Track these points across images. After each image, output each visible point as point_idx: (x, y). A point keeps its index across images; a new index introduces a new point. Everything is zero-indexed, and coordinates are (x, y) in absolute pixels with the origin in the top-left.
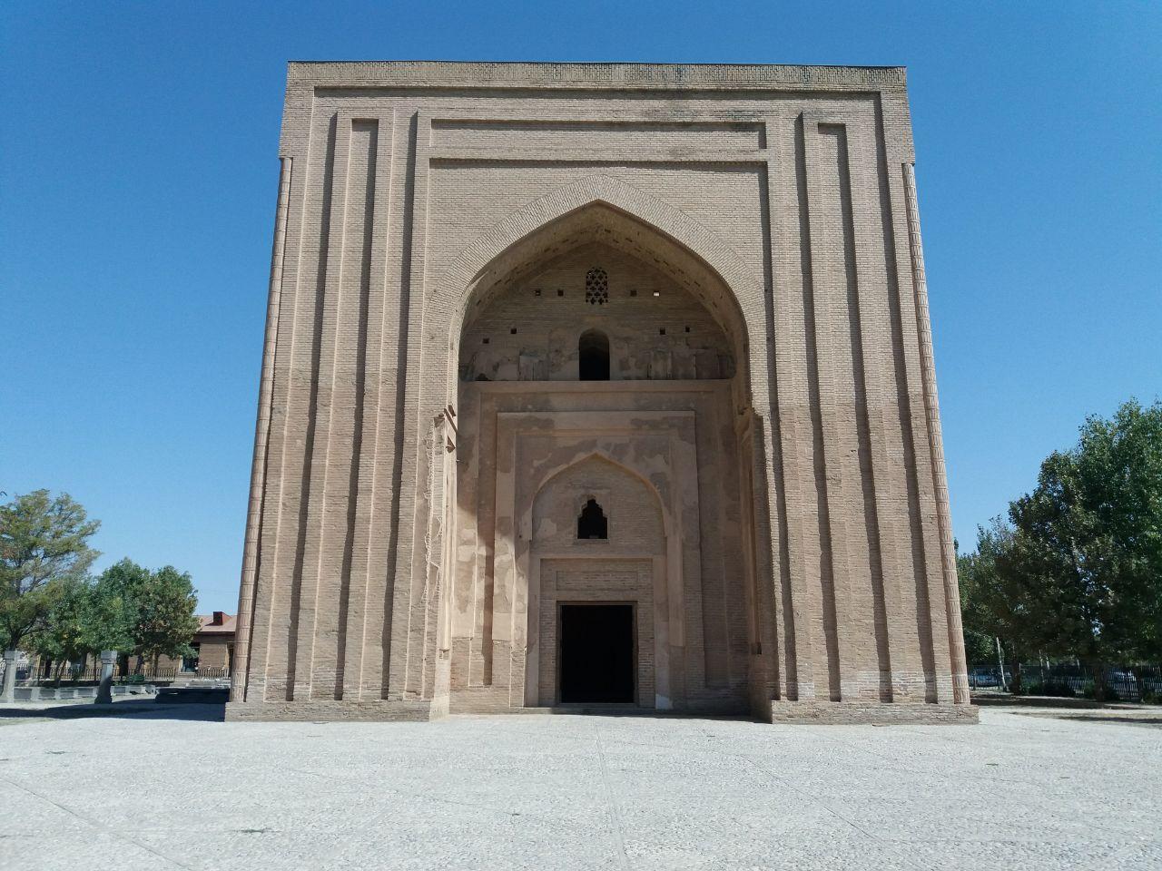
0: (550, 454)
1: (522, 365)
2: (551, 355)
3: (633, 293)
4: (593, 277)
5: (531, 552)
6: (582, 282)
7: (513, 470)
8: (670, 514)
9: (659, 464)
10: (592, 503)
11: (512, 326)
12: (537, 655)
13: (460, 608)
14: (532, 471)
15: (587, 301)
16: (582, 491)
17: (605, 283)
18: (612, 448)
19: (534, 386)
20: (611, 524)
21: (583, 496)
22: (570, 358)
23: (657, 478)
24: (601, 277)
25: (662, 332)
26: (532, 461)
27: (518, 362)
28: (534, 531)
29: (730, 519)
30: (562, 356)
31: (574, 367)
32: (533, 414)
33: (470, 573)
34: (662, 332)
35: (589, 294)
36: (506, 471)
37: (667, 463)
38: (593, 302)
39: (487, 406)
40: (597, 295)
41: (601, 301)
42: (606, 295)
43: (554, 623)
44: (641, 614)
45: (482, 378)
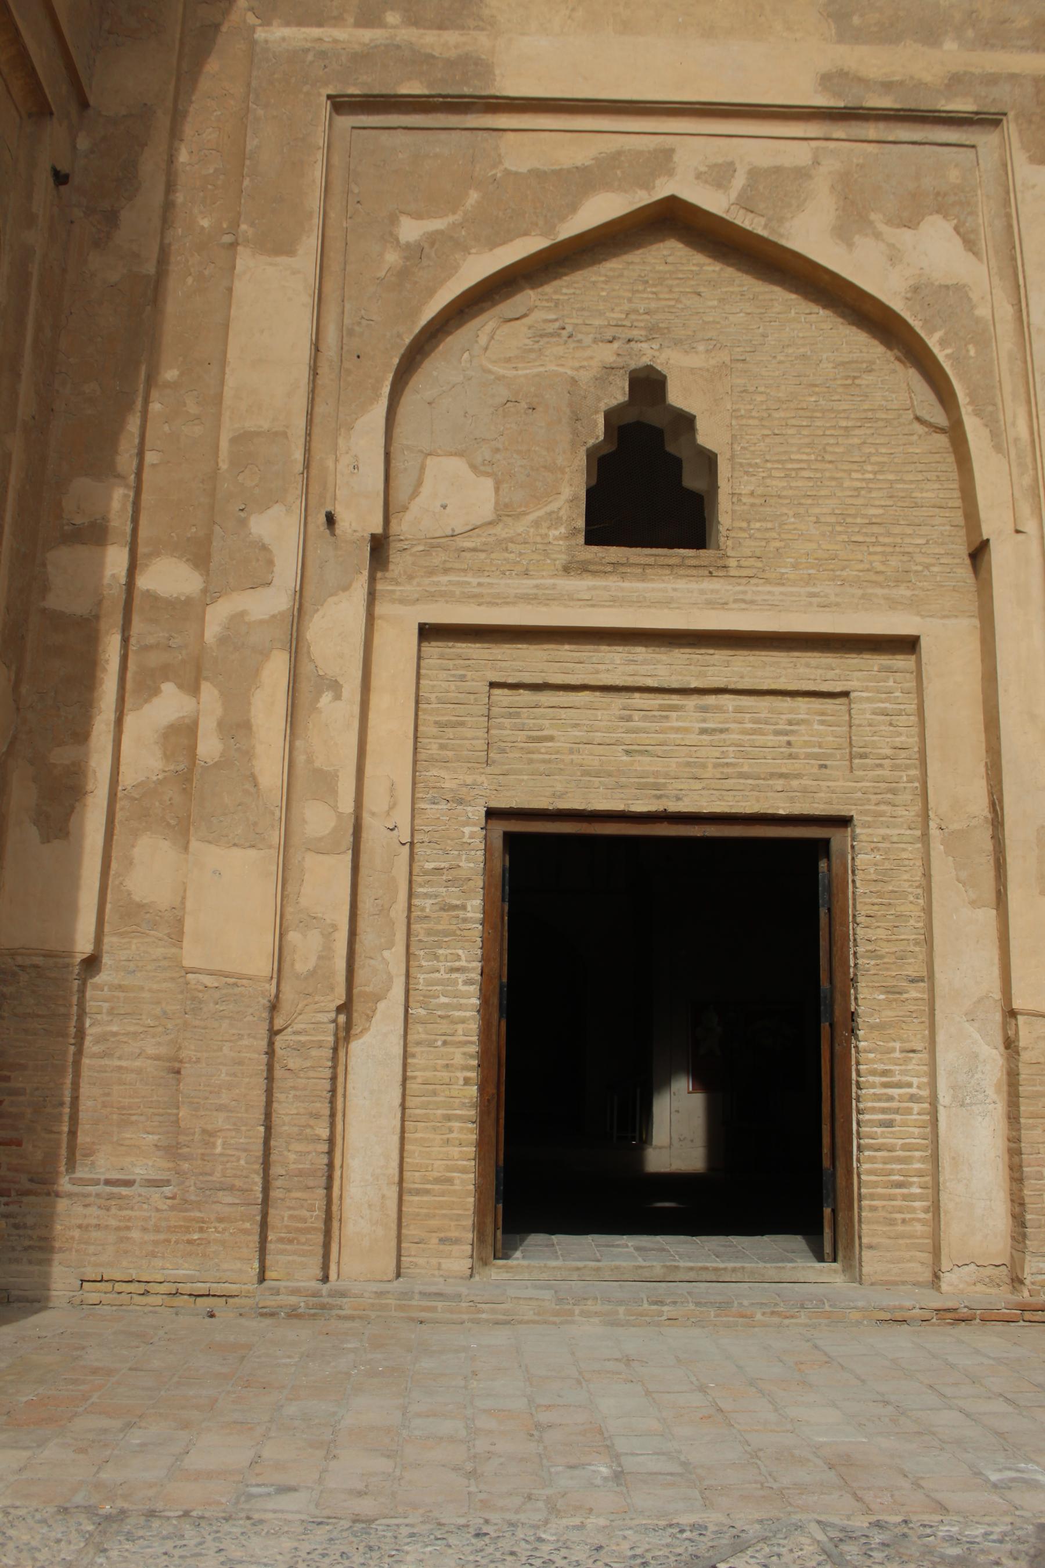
0: (474, 196)
7: (311, 243)
8: (998, 448)
10: (648, 385)
14: (392, 258)
16: (607, 354)
18: (739, 181)
26: (393, 220)
36: (280, 246)
37: (970, 244)
43: (474, 907)
44: (874, 882)
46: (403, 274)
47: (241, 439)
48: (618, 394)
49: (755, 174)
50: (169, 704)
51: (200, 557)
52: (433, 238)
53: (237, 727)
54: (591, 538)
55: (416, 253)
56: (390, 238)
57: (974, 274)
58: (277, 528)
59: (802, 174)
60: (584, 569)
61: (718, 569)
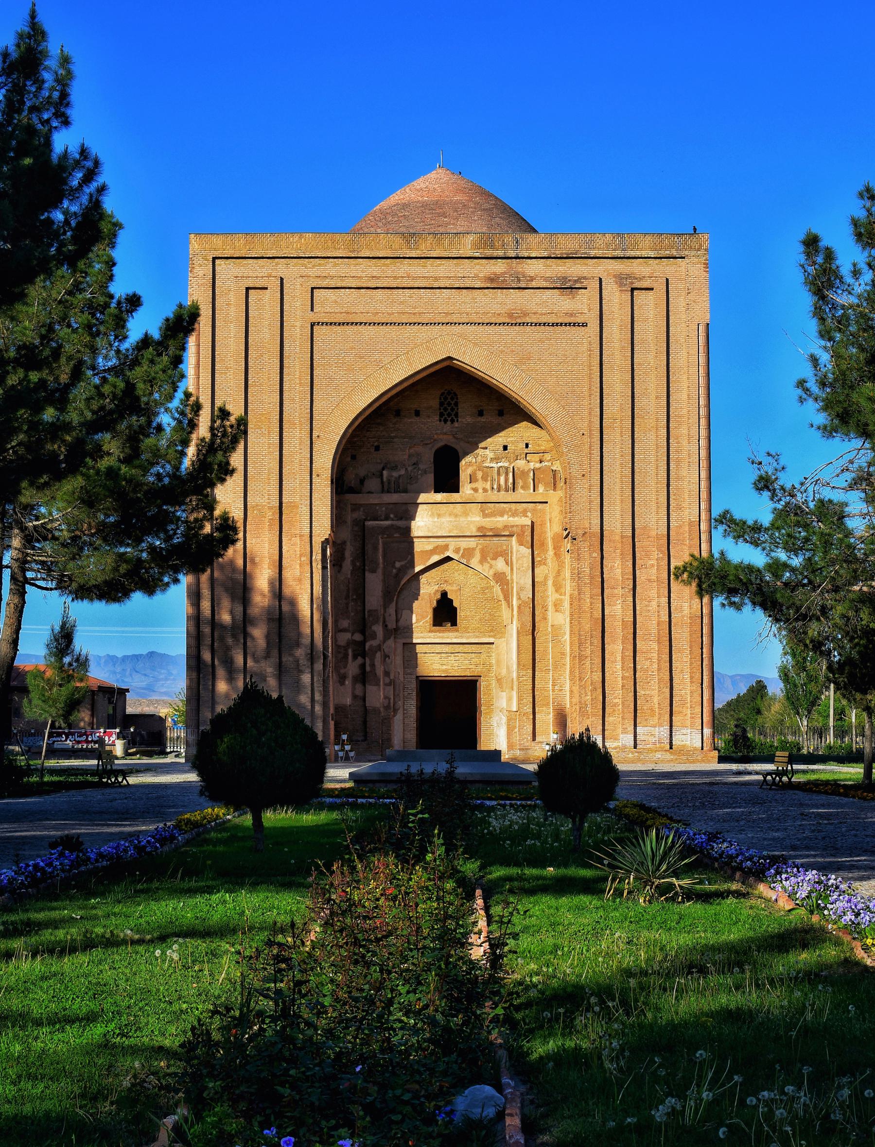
1: (385, 479)
2: (409, 469)
3: (481, 414)
4: (446, 399)
5: (395, 638)
6: (435, 403)
9: (500, 565)
10: (444, 594)
11: (376, 444)
12: (401, 718)
13: (340, 682)
15: (440, 421)
16: (436, 587)
17: (456, 404)
18: (461, 552)
19: (395, 498)
20: (460, 615)
21: (437, 591)
22: (425, 472)
23: (500, 578)
24: (452, 399)
25: (505, 448)
27: (382, 475)
28: (397, 621)
29: (556, 611)
30: (419, 469)
31: (430, 478)
32: (395, 523)
33: (346, 656)
34: (505, 448)
35: (441, 415)
36: (374, 571)
37: (507, 563)
38: (446, 421)
39: (355, 515)
40: (449, 415)
41: (452, 421)
42: (457, 415)
43: (414, 693)
45: (352, 490)
46: (397, 574)
47: (370, 611)
48: (439, 596)
49: (465, 549)
50: (360, 660)
51: (363, 632)
52: (402, 566)
53: (373, 665)
54: (434, 625)
55: (399, 570)
56: (393, 566)
57: (507, 570)
58: (378, 629)
59: (474, 549)
60: (430, 631)
61: (457, 631)
